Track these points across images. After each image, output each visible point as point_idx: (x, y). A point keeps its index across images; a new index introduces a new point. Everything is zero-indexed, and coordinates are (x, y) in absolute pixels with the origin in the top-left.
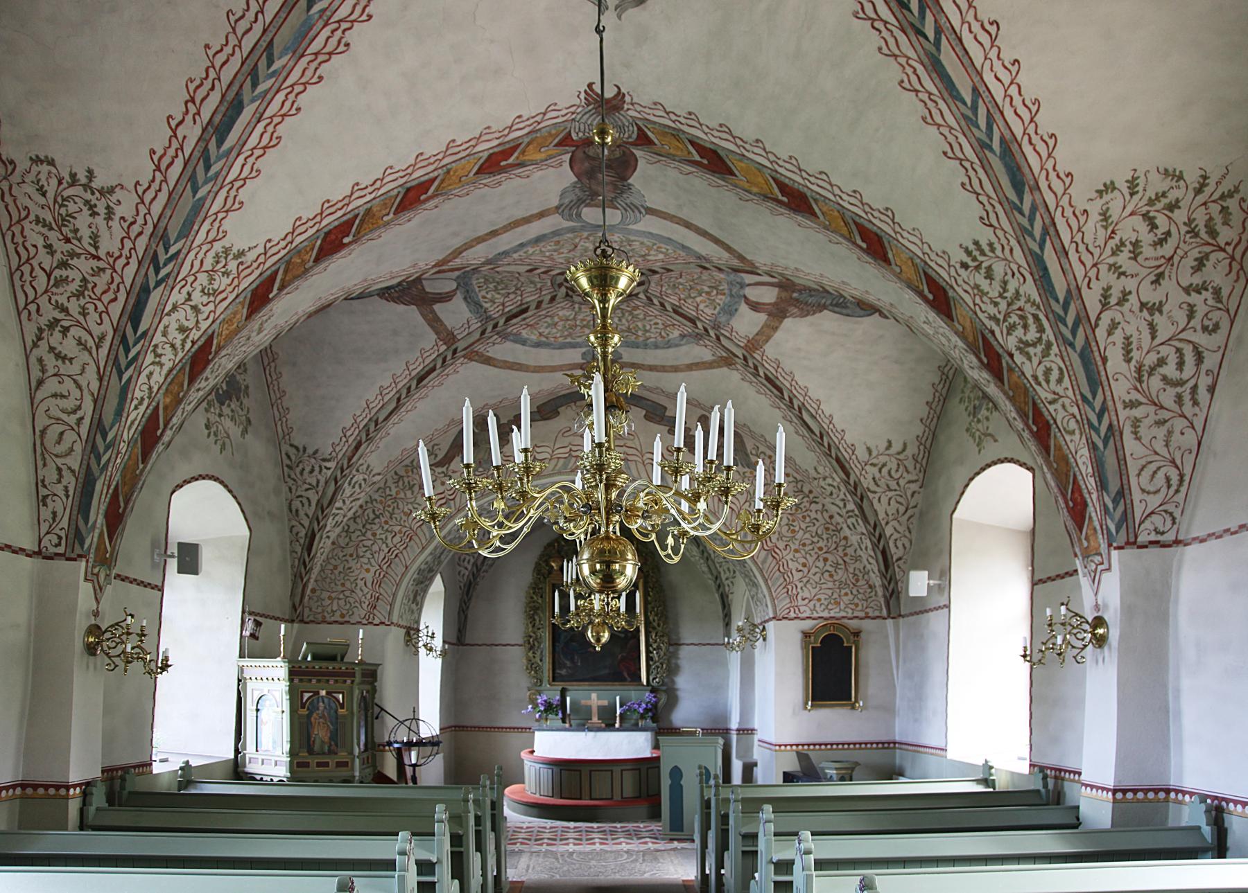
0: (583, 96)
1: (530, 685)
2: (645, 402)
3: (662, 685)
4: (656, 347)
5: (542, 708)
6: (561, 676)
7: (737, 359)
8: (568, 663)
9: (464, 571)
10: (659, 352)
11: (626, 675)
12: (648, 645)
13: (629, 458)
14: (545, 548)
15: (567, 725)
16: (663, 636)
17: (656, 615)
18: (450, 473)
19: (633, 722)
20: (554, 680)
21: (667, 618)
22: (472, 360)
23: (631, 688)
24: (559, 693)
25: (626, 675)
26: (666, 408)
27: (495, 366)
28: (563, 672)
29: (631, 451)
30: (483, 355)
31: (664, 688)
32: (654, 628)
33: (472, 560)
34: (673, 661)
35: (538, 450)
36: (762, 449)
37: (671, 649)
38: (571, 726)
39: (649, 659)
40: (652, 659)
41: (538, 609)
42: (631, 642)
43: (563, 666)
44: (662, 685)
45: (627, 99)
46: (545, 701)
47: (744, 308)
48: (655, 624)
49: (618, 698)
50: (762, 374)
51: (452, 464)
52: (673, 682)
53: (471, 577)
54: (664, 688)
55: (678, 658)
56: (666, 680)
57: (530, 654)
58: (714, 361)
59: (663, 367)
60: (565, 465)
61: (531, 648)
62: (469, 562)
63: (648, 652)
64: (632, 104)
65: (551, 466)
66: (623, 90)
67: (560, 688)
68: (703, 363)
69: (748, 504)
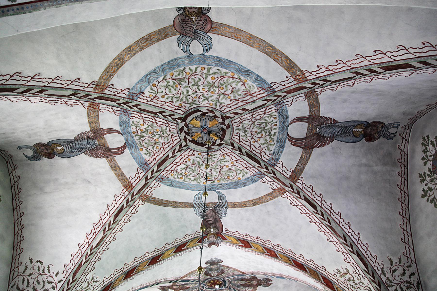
0: (219, 245)
4: (155, 72)
7: (96, 95)
10: (151, 68)
22: (302, 71)
27: (287, 57)
45: (208, 247)
47: (118, 128)
58: (108, 80)
64: (206, 246)
66: (209, 248)
68: (115, 72)
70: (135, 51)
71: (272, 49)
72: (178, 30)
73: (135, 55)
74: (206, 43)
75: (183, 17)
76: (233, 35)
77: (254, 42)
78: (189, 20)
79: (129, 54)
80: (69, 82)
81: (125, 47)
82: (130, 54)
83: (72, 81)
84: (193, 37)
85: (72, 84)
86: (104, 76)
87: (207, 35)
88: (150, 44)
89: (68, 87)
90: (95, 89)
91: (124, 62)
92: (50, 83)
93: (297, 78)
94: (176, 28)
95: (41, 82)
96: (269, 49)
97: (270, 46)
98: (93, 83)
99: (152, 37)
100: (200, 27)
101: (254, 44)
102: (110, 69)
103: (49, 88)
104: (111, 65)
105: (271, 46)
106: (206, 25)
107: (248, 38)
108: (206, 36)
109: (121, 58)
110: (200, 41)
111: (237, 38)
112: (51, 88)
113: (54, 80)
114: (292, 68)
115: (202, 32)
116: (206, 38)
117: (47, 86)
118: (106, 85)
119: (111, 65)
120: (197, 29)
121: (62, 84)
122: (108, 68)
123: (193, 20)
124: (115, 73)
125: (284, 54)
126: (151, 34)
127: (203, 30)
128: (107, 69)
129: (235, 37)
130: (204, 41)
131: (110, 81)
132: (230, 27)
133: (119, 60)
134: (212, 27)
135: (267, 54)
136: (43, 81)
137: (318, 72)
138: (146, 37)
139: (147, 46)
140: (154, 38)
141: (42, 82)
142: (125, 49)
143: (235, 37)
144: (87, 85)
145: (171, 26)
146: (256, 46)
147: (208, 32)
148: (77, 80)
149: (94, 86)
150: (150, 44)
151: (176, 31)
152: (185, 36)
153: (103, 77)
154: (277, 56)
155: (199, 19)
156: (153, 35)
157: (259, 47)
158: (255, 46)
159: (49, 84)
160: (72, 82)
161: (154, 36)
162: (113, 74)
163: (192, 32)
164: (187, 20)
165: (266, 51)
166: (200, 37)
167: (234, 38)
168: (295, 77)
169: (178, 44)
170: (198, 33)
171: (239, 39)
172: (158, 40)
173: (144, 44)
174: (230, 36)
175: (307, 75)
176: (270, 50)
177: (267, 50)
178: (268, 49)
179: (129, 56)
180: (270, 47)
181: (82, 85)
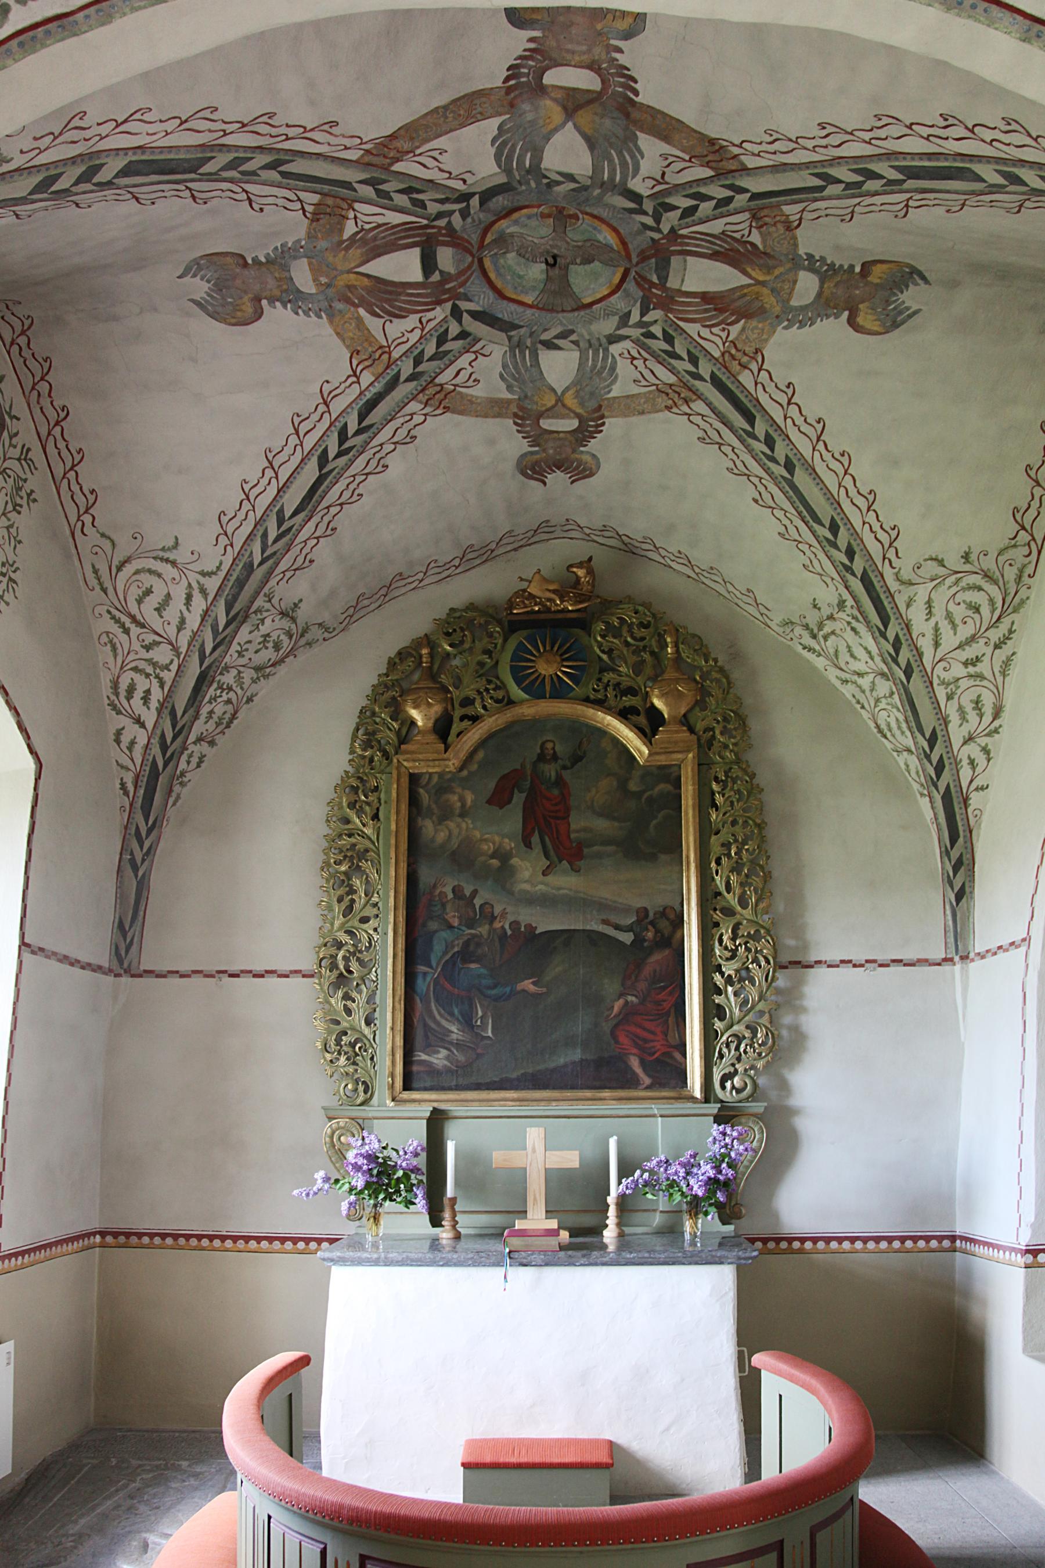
1: (333, 1102)
3: (752, 1097)
5: (359, 1181)
6: (432, 1071)
8: (455, 1031)
9: (132, 731)
11: (635, 1063)
12: (709, 967)
14: (392, 664)
15: (445, 1234)
16: (756, 937)
17: (736, 869)
19: (657, 1220)
20: (407, 1086)
21: (768, 877)
23: (655, 1108)
24: (421, 1128)
25: (635, 1063)
28: (439, 1059)
31: (758, 1107)
32: (729, 912)
33: (157, 695)
34: (787, 1019)
37: (782, 980)
38: (458, 1237)
39: (712, 1011)
40: (720, 1012)
41: (363, 855)
42: (657, 957)
43: (438, 1039)
44: (752, 1097)
46: (371, 1158)
48: (732, 900)
49: (613, 1143)
52: (784, 1087)
53: (156, 750)
54: (758, 1107)
55: (804, 1010)
56: (761, 1081)
57: (337, 1002)
61: (342, 980)
62: (146, 699)
63: (709, 989)
67: (426, 1110)
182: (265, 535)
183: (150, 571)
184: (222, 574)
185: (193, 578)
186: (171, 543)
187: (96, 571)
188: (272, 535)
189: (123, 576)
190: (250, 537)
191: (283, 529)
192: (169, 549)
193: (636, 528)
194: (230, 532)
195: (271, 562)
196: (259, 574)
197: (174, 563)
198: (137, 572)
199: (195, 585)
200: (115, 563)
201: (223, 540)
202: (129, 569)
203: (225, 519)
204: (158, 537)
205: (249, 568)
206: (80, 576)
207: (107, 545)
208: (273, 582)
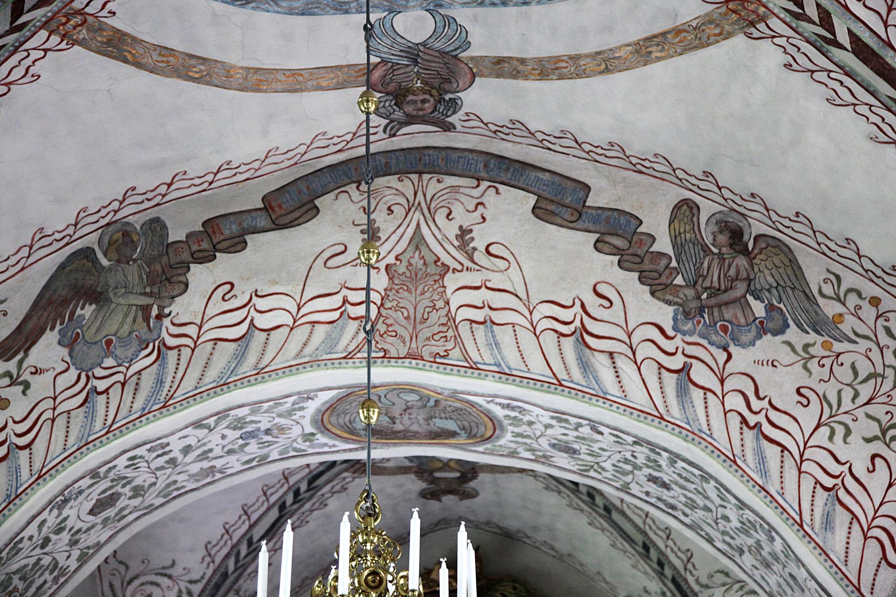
2: (533, 174)
13: (497, 317)
18: (26, 376)
22: (75, 42)
26: (587, 188)
27: (138, 65)
29: (499, 299)
30: (101, 28)
35: (262, 304)
36: (850, 280)
50: (843, 37)
51: (34, 351)
58: (709, 20)
59: (575, 58)
60: (330, 343)
65: (293, 347)
68: (678, 31)
69: (824, 431)
70: (595, 60)
71: (190, 74)
72: (463, 66)
73: (599, 50)
74: (384, 39)
75: (446, 86)
76: (307, 76)
77: (245, 79)
78: (432, 80)
79: (615, 58)
80: (822, 76)
81: (619, 76)
82: (611, 56)
83: (810, 73)
84: (422, 48)
85: (814, 68)
86: (715, 35)
87: (381, 57)
88: (549, 62)
89: (832, 67)
90: (763, 19)
91: (638, 44)
92: (867, 104)
93: (78, 19)
94: (468, 71)
95: (886, 121)
96: (196, 72)
97: (197, 78)
98: (756, 34)
99: (538, 72)
100: (402, 71)
101: (243, 75)
102: (686, 43)
103: (881, 99)
104: (679, 50)
105: (194, 80)
106: (385, 76)
107: (265, 81)
108: (383, 55)
109: (642, 56)
110: (403, 41)
111: (295, 73)
112: (876, 95)
113: (853, 104)
114: (109, 43)
115: (394, 61)
116: (386, 50)
117: (880, 105)
118: (724, 9)
119: (679, 50)
120: (408, 66)
121: (842, 83)
122: (691, 46)
123: (419, 81)
124: (680, 28)
125: (151, 72)
126: (538, 78)
127: (392, 66)
128: (696, 48)
129: (301, 75)
130: (389, 42)
131: (707, 15)
132: (320, 88)
133: (650, 52)
134: (366, 76)
135: (199, 58)
136: (880, 119)
137: (28, 62)
138: (555, 77)
139: (558, 59)
140: (534, 69)
141: (883, 119)
142: (620, 71)
143: (301, 75)
144: (776, 40)
145: (481, 76)
146: (237, 73)
147: (379, 63)
148: (795, 66)
149: (761, 26)
150: (549, 62)
151: (471, 66)
152: (447, 53)
153: (720, 34)
154: (168, 62)
155: (402, 84)
156: (533, 74)
157: (228, 71)
158: (241, 71)
159: (872, 106)
160: (813, 72)
161: (533, 72)
162: (686, 27)
163: (423, 59)
164: (436, 80)
165: (202, 64)
166: (401, 51)
167: (302, 72)
168: (85, 21)
169: (469, 39)
170: (406, 57)
171: (288, 73)
172: (522, 61)
173: (564, 64)
174: (316, 71)
175: (55, 39)
176: (195, 70)
177: (203, 67)
178: (201, 71)
179: (617, 55)
180: (197, 76)
181: (790, 49)
182: (238, 553)
183: (152, 583)
184: (204, 581)
185: (183, 585)
186: (169, 563)
187: (111, 586)
188: (244, 552)
189: (130, 589)
190: (227, 556)
191: (252, 548)
192: (168, 568)
193: (512, 524)
194: (213, 552)
195: (240, 570)
196: (231, 579)
197: (170, 577)
198: (142, 584)
199: (184, 590)
200: (127, 578)
201: (208, 559)
202: (136, 583)
203: (209, 546)
204: (160, 559)
205: (225, 575)
206: (99, 590)
207: (122, 569)
208: (241, 582)
